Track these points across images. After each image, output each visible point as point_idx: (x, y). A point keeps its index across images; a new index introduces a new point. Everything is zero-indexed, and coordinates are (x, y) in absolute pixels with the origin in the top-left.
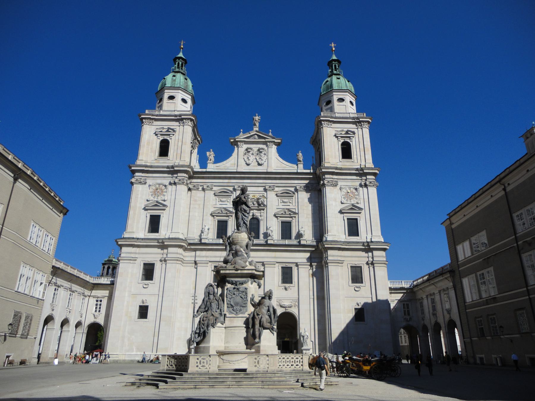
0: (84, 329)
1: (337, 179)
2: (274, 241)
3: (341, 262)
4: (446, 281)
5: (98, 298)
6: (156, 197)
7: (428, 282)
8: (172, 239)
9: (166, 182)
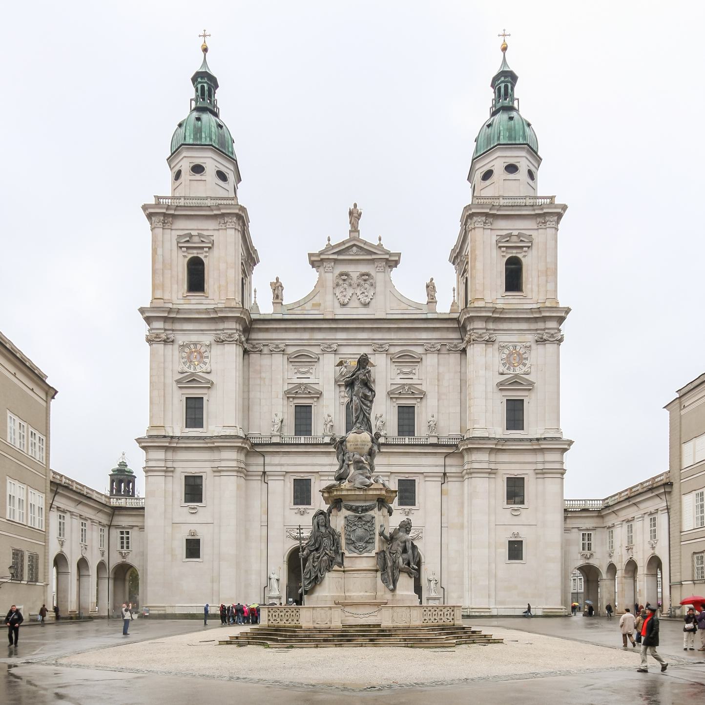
0: (108, 573)
1: (495, 330)
2: (387, 439)
3: (492, 472)
4: (657, 500)
5: (124, 528)
6: (192, 366)
7: (628, 501)
8: (226, 437)
9: (208, 339)
